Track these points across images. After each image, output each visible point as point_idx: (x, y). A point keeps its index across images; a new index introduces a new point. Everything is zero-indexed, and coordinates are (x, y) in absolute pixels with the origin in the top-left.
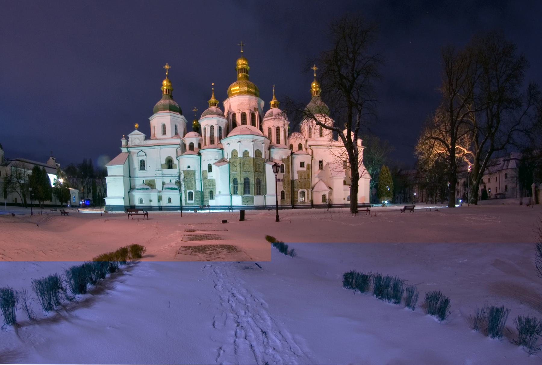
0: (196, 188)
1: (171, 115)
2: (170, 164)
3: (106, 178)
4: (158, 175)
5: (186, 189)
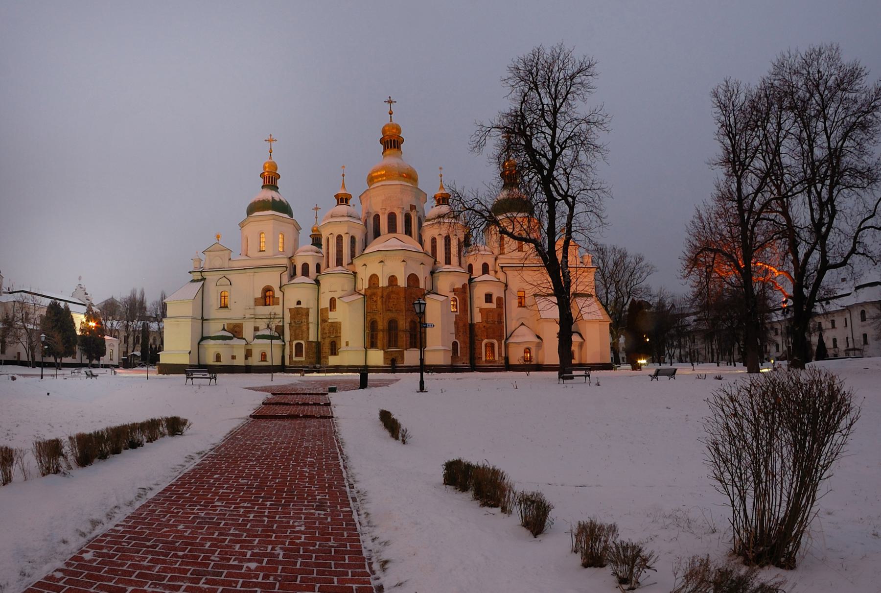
0: (308, 338)
2: (267, 297)
4: (247, 316)
5: (293, 339)
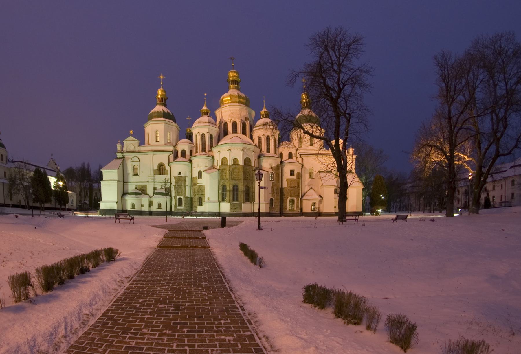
0: (185, 194)
1: (164, 123)
2: (161, 169)
3: (101, 182)
4: (150, 181)
5: (176, 195)
